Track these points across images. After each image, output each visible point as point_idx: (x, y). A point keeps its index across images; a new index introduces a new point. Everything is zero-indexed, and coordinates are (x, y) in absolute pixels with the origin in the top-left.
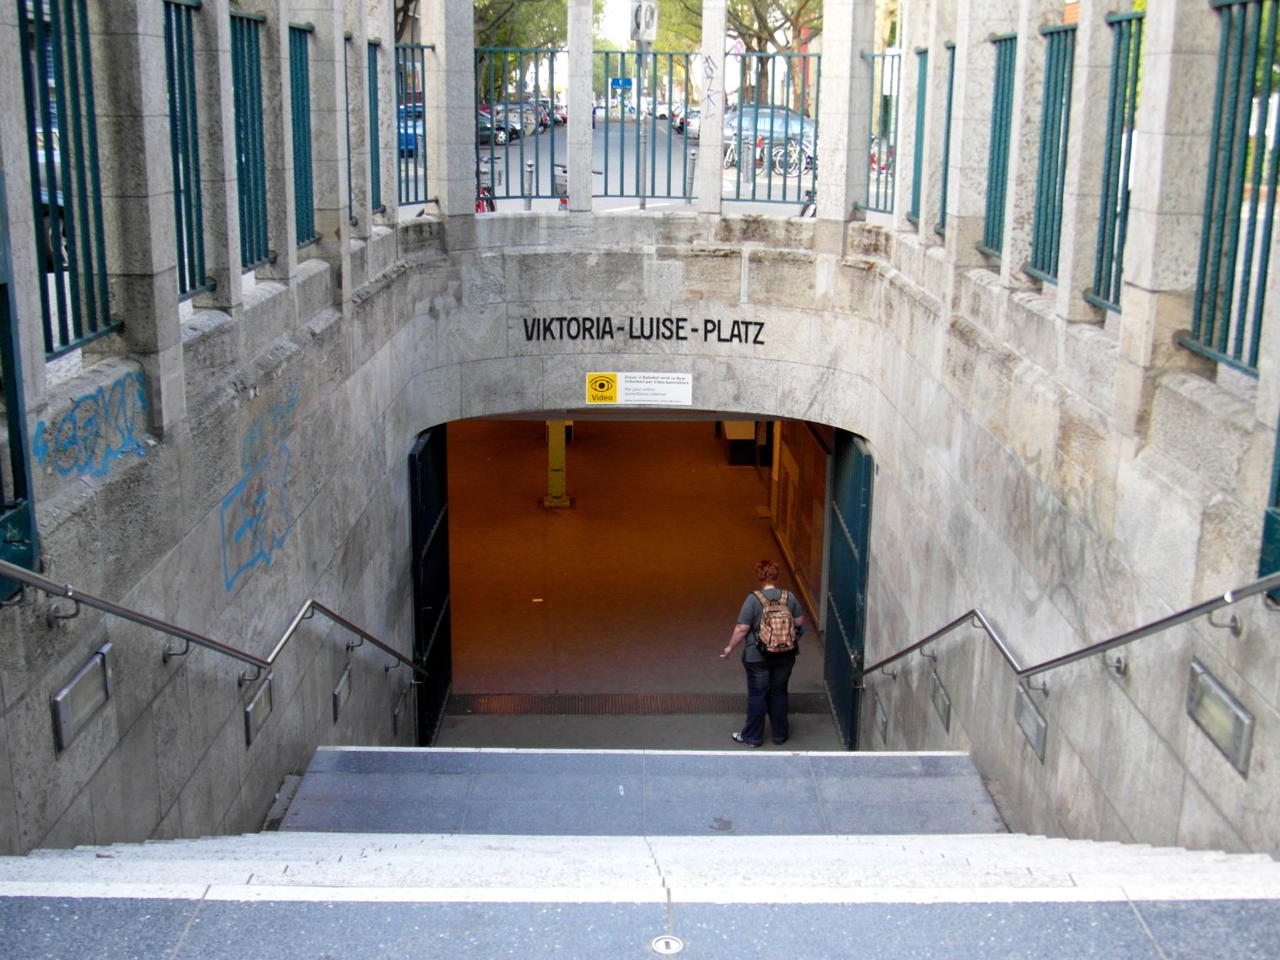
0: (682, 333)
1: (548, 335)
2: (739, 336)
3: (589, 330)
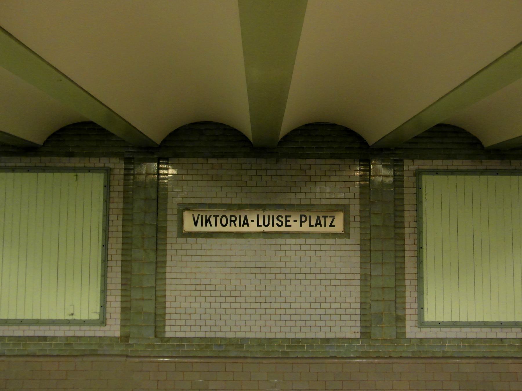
0: (288, 224)
3: (234, 221)
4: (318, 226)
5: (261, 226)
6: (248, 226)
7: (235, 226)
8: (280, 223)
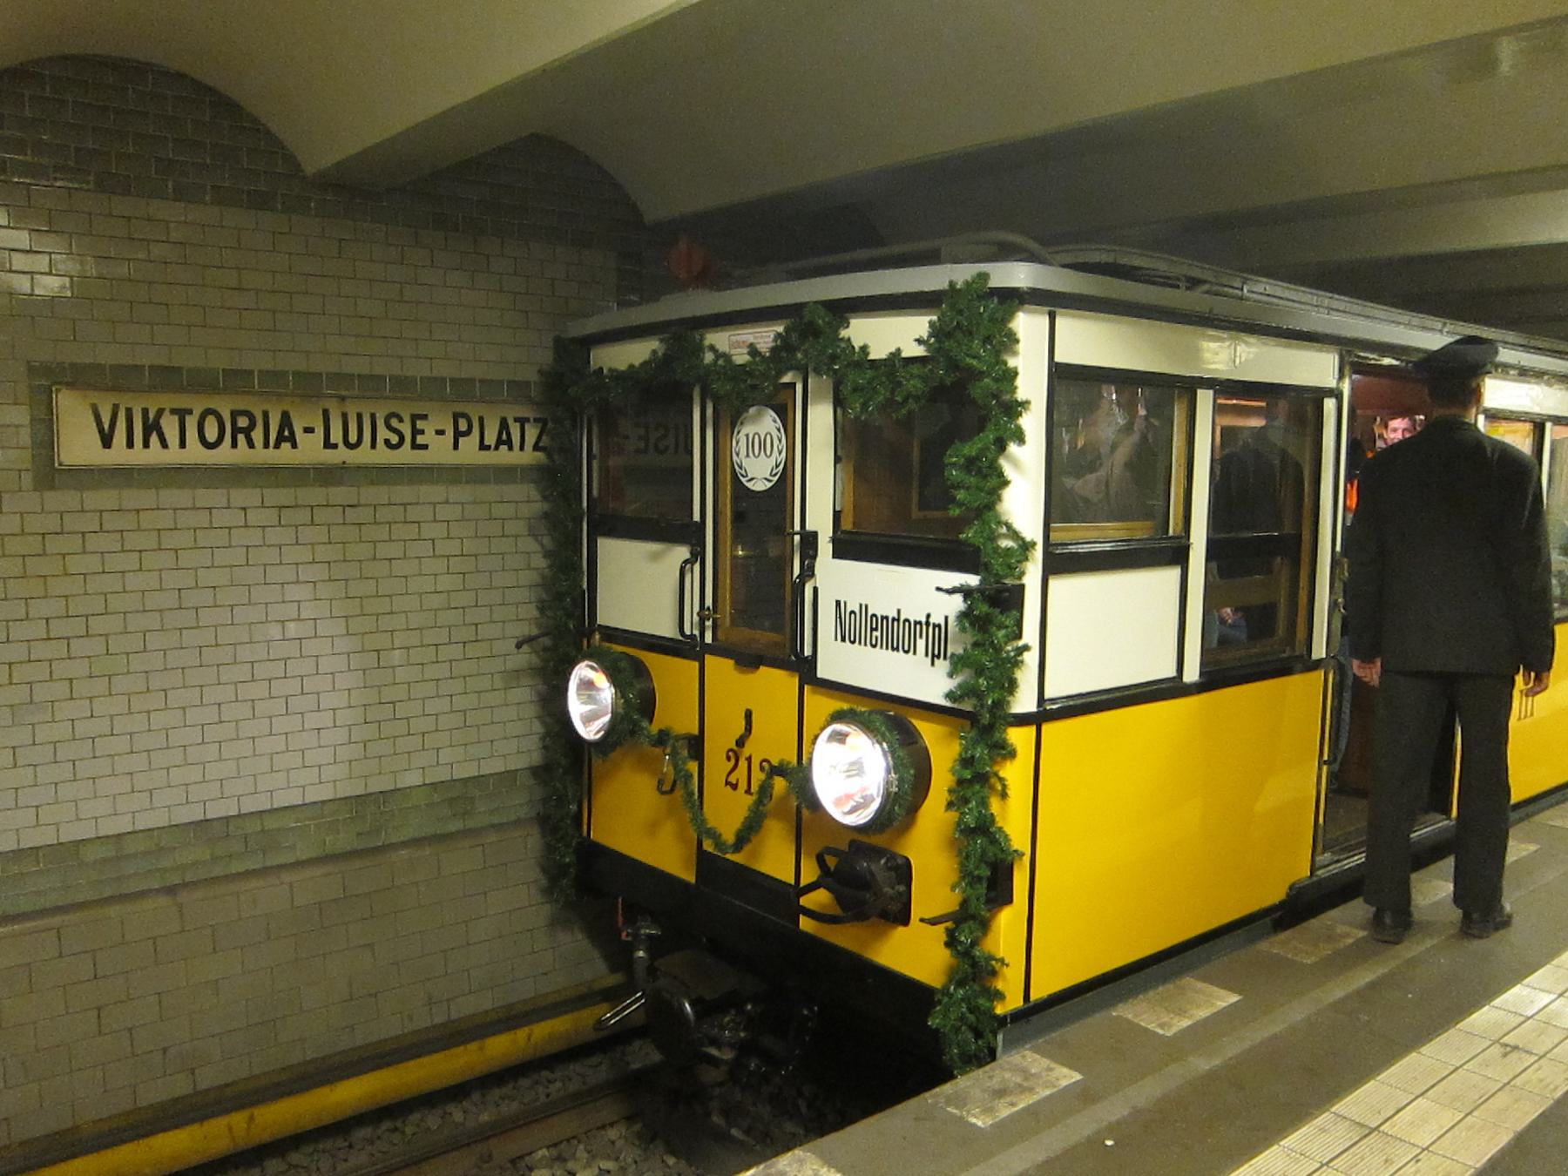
0: (420, 440)
1: (154, 439)
2: (509, 444)
3: (247, 431)
4: (504, 448)
5: (335, 446)
6: (294, 446)
7: (251, 445)
8: (395, 439)
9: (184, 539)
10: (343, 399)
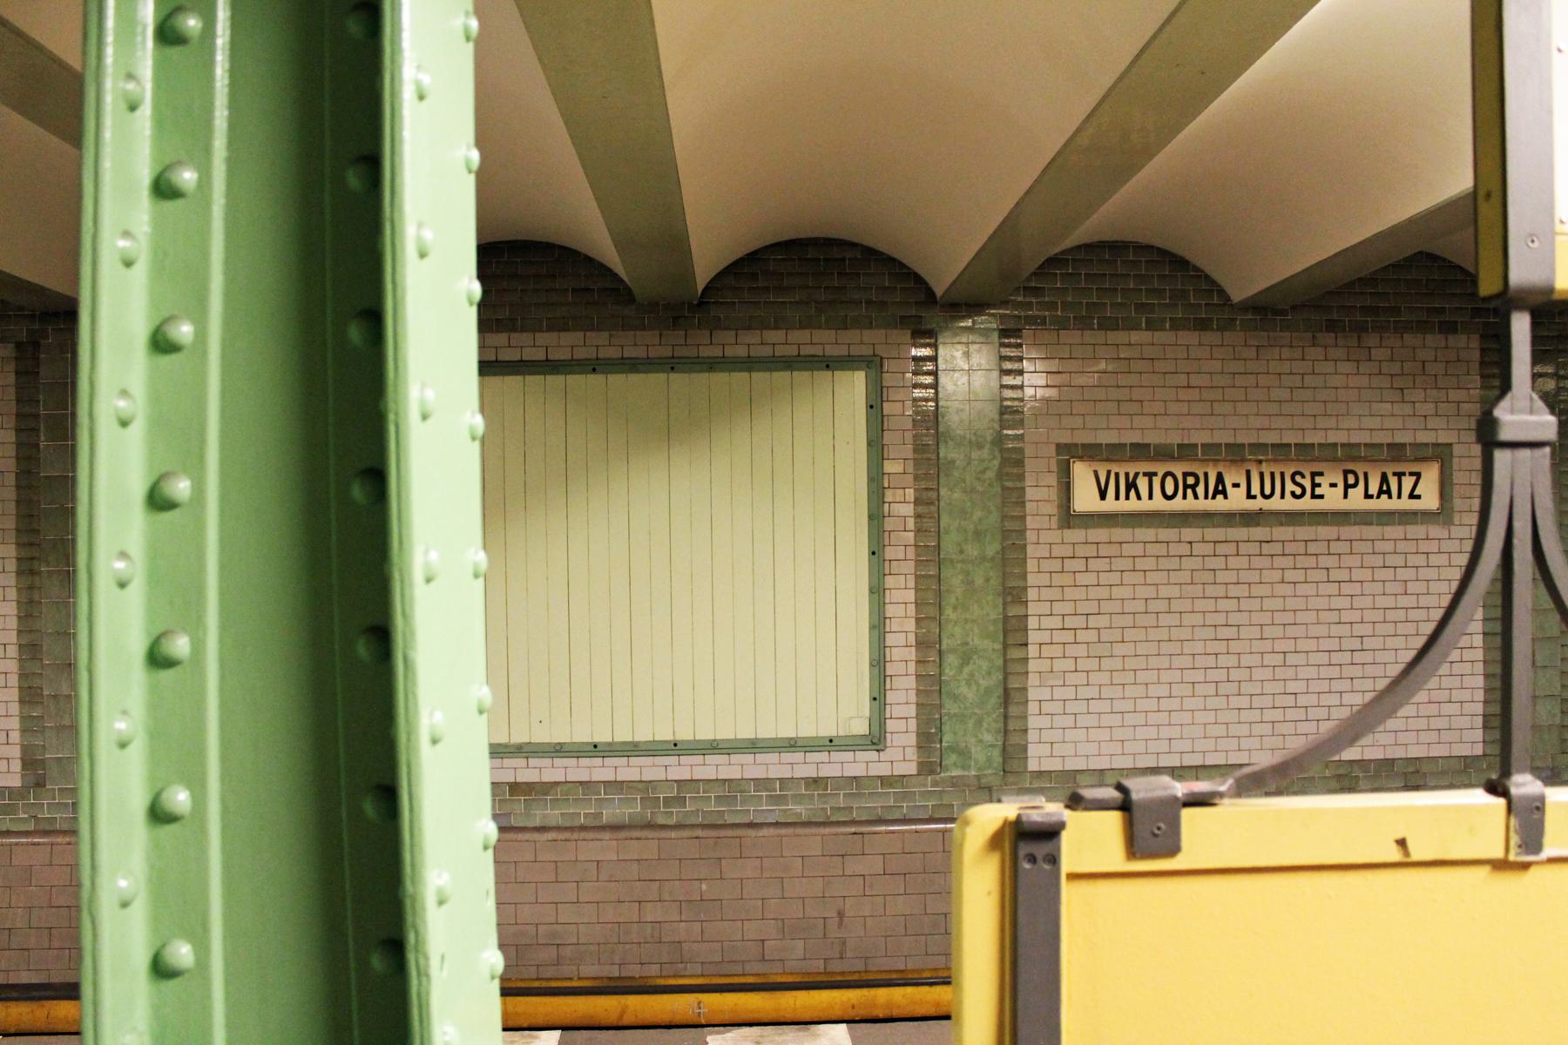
0: (1318, 491)
3: (1194, 487)
4: (1384, 497)
7: (1196, 497)
8: (1298, 491)
9: (1149, 563)
10: (1260, 462)
